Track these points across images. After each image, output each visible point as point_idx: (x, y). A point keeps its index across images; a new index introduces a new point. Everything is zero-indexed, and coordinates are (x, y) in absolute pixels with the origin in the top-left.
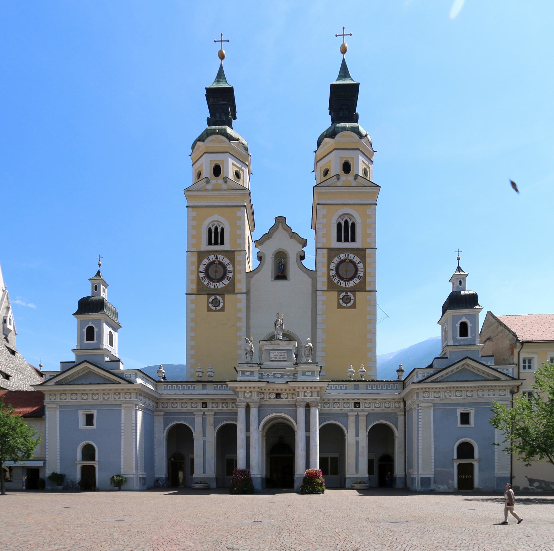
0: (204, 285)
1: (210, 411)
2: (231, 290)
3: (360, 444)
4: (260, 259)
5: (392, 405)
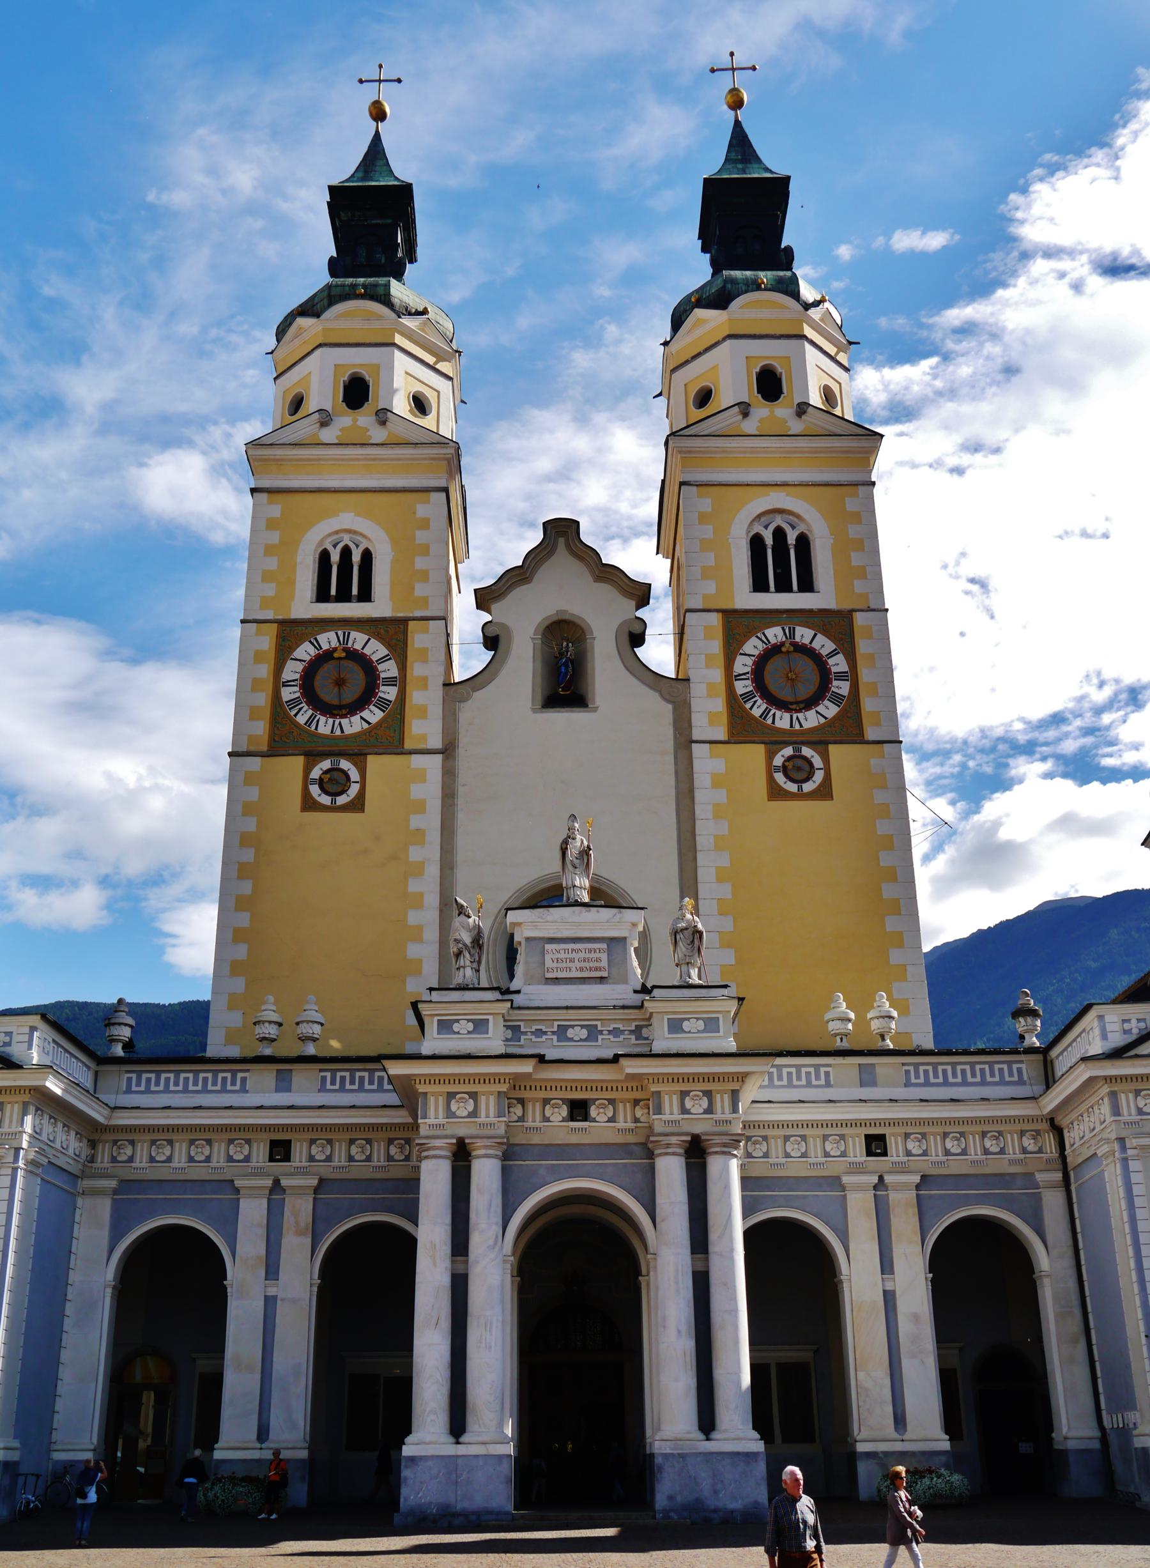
0: (297, 724)
1: (299, 1177)
2: (390, 738)
3: (903, 1307)
4: (491, 641)
5: (1012, 1143)
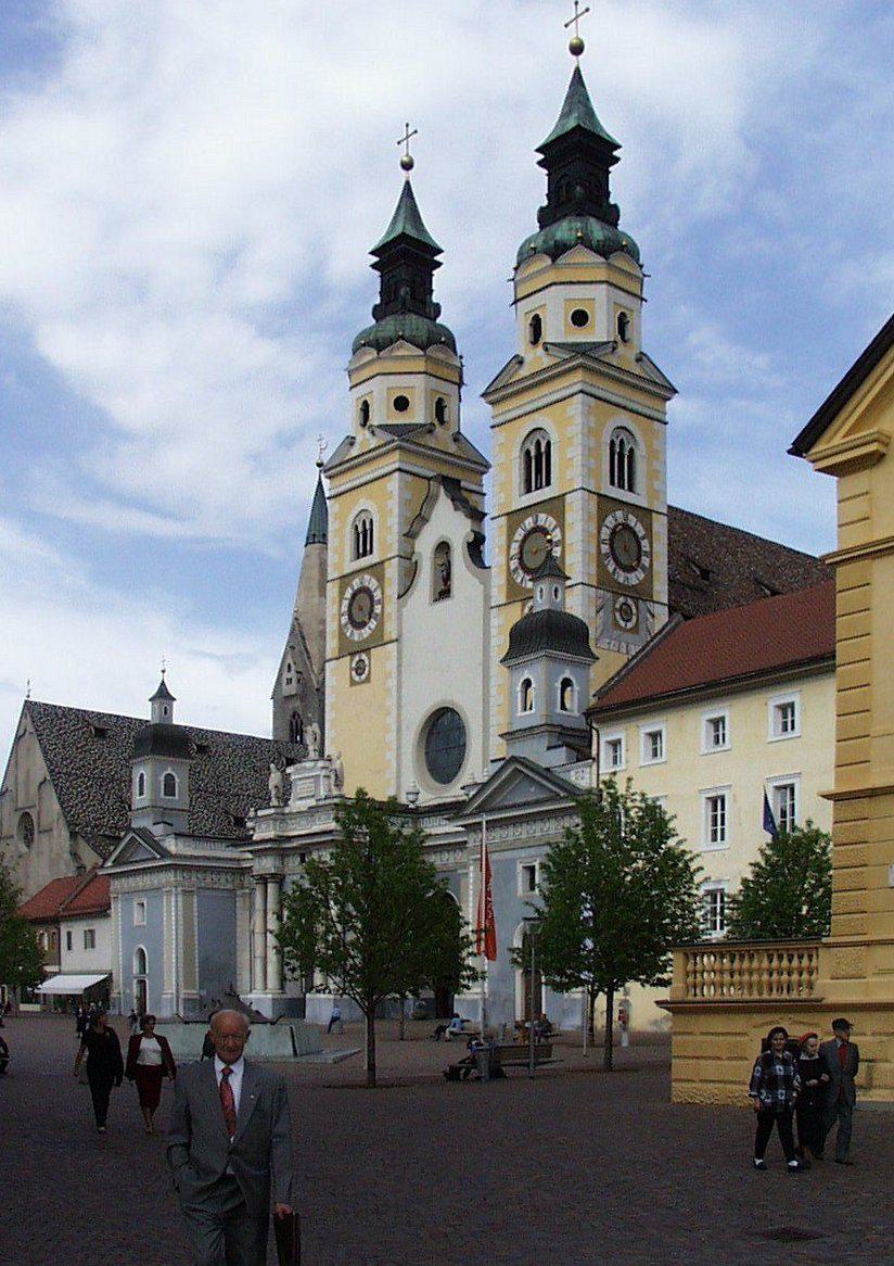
2: (378, 640)
